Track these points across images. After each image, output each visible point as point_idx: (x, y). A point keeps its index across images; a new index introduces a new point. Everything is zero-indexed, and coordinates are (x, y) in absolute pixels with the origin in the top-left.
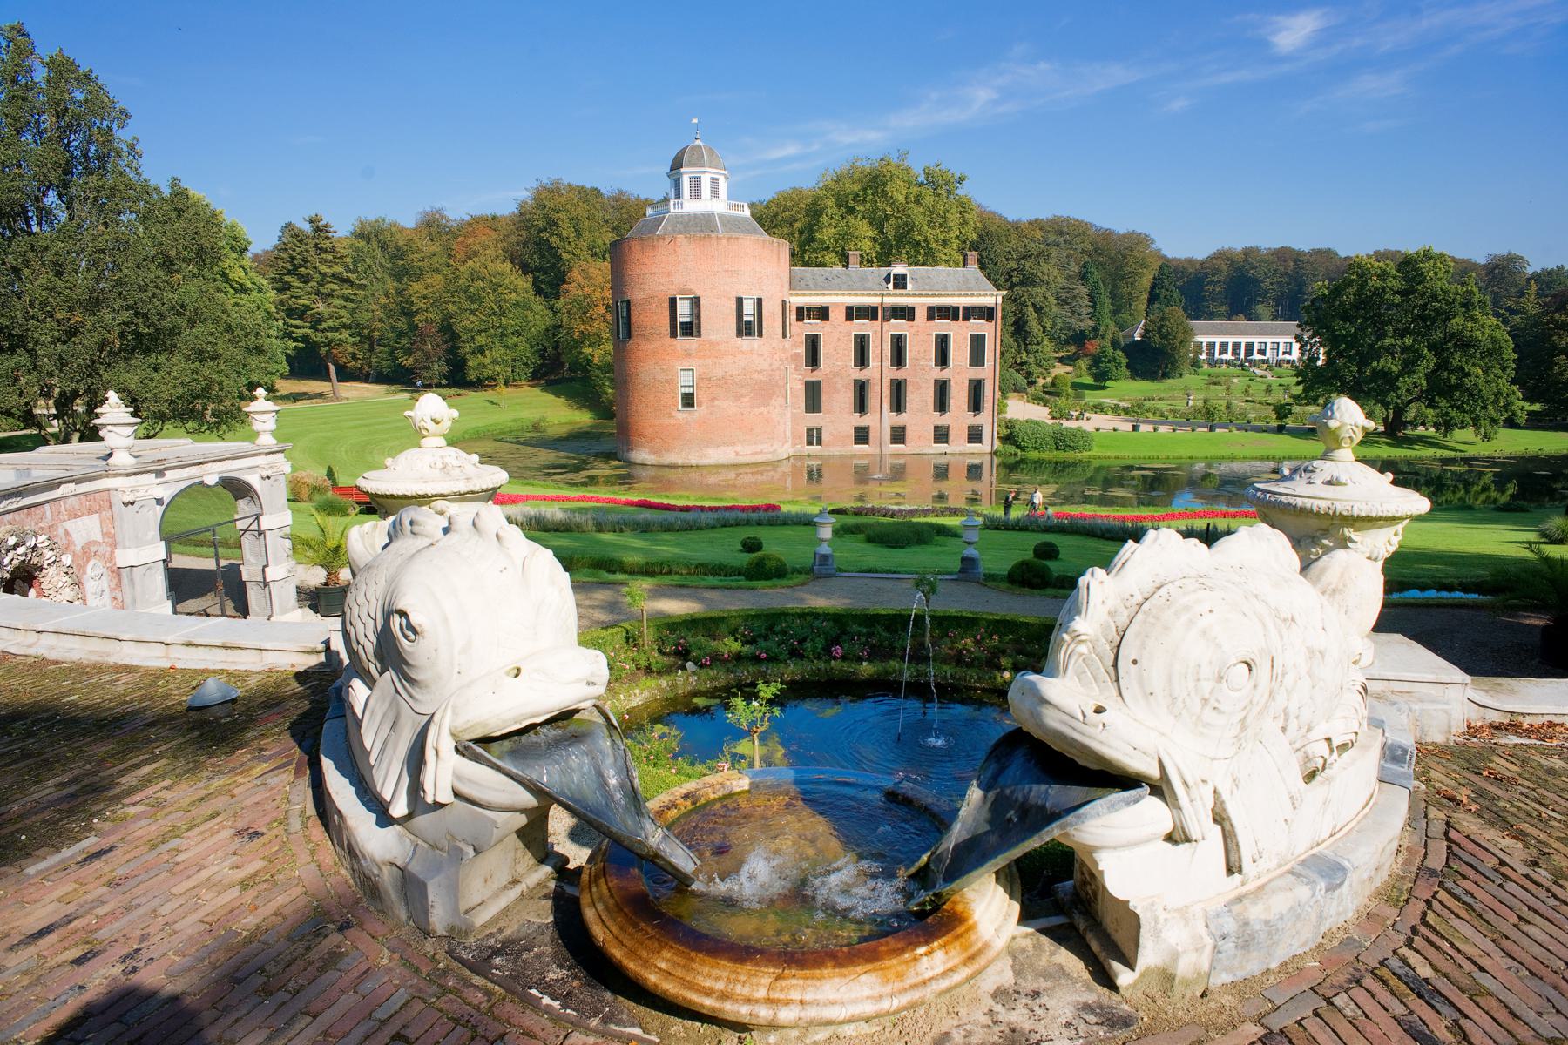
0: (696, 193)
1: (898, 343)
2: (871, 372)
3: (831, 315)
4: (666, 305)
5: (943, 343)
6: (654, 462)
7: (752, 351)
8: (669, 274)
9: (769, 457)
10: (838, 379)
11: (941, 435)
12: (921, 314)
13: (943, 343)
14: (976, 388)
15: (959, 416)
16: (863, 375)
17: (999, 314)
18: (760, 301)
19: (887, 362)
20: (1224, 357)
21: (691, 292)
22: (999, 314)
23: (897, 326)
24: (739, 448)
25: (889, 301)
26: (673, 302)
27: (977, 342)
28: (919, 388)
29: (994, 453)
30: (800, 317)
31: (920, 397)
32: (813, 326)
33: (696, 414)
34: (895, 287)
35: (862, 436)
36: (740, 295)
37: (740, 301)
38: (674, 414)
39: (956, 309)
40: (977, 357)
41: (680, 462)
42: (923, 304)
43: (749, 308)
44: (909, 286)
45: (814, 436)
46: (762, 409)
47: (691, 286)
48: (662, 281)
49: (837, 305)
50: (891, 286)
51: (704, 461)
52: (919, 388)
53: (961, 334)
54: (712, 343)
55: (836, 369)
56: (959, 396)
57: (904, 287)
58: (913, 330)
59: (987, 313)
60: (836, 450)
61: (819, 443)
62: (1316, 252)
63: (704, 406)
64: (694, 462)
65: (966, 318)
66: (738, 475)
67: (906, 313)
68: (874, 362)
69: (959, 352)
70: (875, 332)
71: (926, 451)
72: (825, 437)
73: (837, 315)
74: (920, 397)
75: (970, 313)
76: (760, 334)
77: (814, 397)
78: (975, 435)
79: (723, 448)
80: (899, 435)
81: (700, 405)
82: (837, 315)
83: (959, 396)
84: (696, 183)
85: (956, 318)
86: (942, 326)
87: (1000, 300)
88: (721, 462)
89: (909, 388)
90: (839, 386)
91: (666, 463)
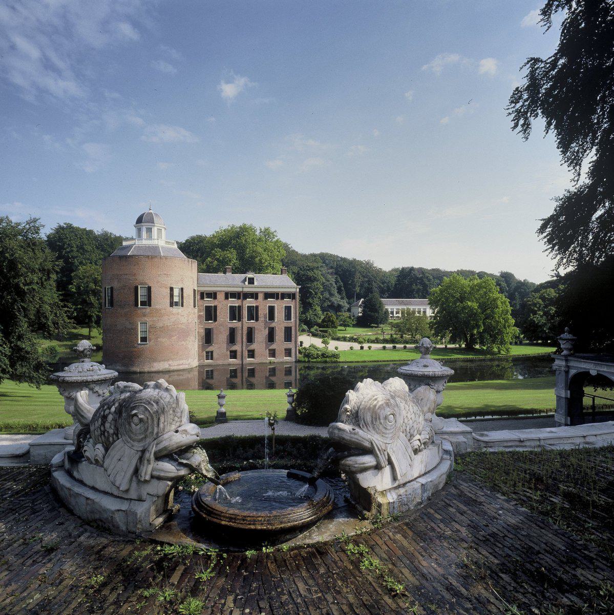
0: (150, 237)
3: (218, 296)
4: (133, 290)
5: (271, 309)
7: (178, 314)
8: (135, 275)
9: (186, 367)
12: (261, 296)
13: (271, 309)
14: (288, 331)
15: (280, 344)
17: (298, 297)
18: (182, 289)
20: (397, 315)
21: (146, 284)
22: (298, 297)
23: (250, 302)
24: (170, 362)
25: (246, 290)
27: (288, 309)
29: (298, 361)
30: (202, 297)
31: (261, 335)
32: (209, 302)
34: (249, 283)
36: (172, 286)
37: (172, 289)
39: (278, 294)
40: (288, 317)
42: (261, 292)
43: (176, 292)
45: (210, 355)
46: (183, 342)
50: (247, 283)
51: (153, 370)
53: (279, 306)
54: (157, 309)
56: (280, 335)
57: (253, 283)
59: (292, 296)
60: (220, 362)
61: (212, 359)
62: (433, 270)
65: (283, 298)
66: (170, 377)
67: (254, 296)
69: (279, 315)
71: (264, 361)
72: (215, 355)
73: (221, 297)
74: (261, 335)
75: (284, 296)
76: (182, 306)
77: (208, 337)
80: (252, 354)
81: (150, 341)
82: (221, 297)
83: (280, 335)
85: (277, 298)
86: (271, 302)
87: (298, 290)
88: (161, 369)
89: (256, 332)
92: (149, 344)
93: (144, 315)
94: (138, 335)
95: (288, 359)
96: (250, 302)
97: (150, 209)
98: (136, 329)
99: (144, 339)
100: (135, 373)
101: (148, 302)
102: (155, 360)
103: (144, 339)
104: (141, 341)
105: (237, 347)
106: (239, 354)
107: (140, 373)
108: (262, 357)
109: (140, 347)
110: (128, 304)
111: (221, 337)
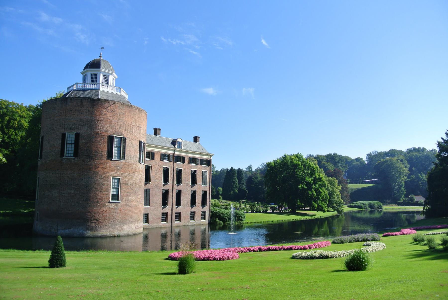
1: (179, 172)
2: (169, 187)
3: (156, 157)
8: (111, 122)
11: (193, 216)
13: (194, 175)
16: (166, 187)
19: (175, 182)
24: (136, 224)
35: (165, 217)
38: (107, 204)
40: (204, 183)
41: (108, 234)
47: (122, 131)
48: (105, 125)
49: (157, 152)
51: (122, 233)
58: (184, 167)
60: (154, 225)
63: (124, 200)
64: (116, 234)
65: (201, 164)
67: (182, 159)
68: (170, 181)
71: (187, 224)
72: (150, 218)
78: (204, 216)
79: (131, 224)
80: (178, 216)
84: (106, 79)
89: (182, 194)
91: (100, 235)
92: (121, 203)
93: (118, 170)
94: (110, 192)
95: (204, 222)
96: (179, 165)
98: (107, 185)
99: (116, 197)
100: (104, 237)
101: (122, 155)
102: (125, 222)
103: (116, 197)
104: (112, 199)
105: (168, 210)
107: (110, 237)
109: (110, 205)
111: (157, 198)
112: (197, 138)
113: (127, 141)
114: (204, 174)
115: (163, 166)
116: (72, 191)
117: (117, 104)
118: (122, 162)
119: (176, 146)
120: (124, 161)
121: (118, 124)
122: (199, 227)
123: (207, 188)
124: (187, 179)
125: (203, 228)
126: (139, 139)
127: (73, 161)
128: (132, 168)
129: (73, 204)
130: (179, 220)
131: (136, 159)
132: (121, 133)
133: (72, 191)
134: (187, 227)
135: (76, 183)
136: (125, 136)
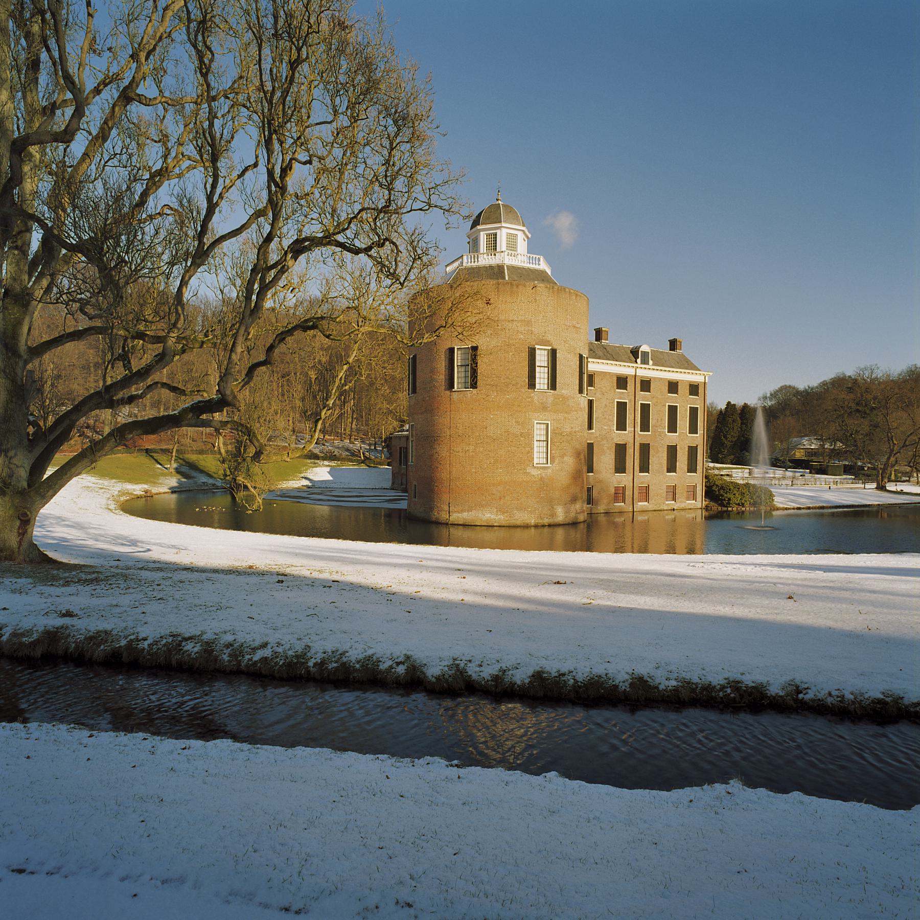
1: (645, 409)
4: (525, 355)
6: (504, 523)
10: (605, 442)
14: (693, 451)
19: (638, 428)
26: (532, 353)
28: (658, 452)
33: (550, 471)
38: (529, 470)
40: (693, 429)
44: (651, 362)
47: (549, 337)
48: (520, 329)
49: (604, 374)
52: (658, 452)
55: (604, 432)
58: (655, 400)
63: (557, 462)
68: (629, 428)
70: (630, 401)
71: (662, 508)
80: (645, 493)
89: (651, 452)
90: (605, 448)
95: (692, 504)
97: (497, 200)
106: (628, 493)
108: (659, 501)
110: (514, 382)
112: (678, 343)
113: (558, 355)
114: (694, 412)
115: (616, 400)
116: (472, 448)
117: (540, 287)
118: (551, 394)
119: (639, 360)
120: (556, 392)
121: (542, 326)
122: (683, 513)
123: (699, 439)
124: (659, 423)
125: (690, 515)
126: (578, 351)
127: (469, 395)
128: (569, 405)
129: (474, 470)
130: (647, 500)
131: (575, 387)
132: (549, 341)
133: (472, 448)
134: (661, 513)
135: (478, 434)
136: (555, 347)
